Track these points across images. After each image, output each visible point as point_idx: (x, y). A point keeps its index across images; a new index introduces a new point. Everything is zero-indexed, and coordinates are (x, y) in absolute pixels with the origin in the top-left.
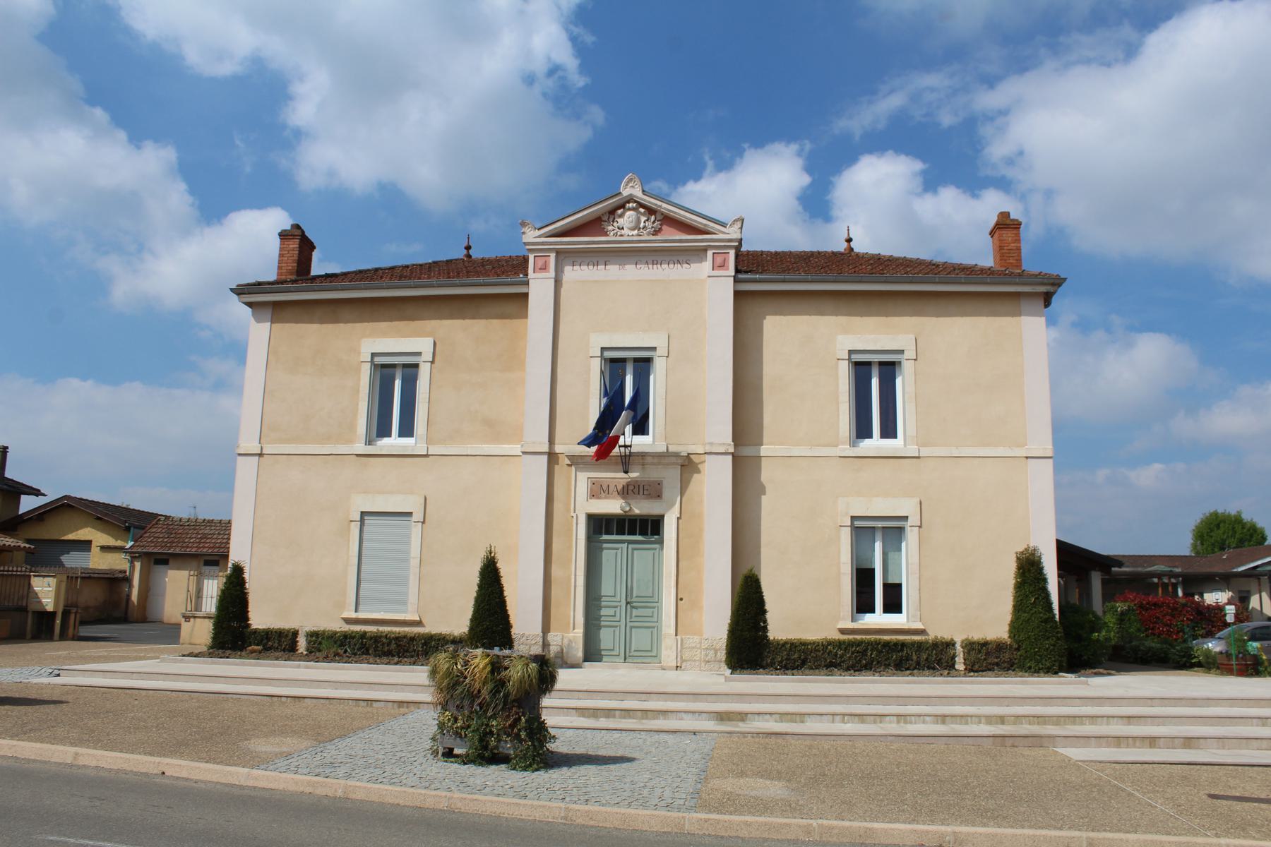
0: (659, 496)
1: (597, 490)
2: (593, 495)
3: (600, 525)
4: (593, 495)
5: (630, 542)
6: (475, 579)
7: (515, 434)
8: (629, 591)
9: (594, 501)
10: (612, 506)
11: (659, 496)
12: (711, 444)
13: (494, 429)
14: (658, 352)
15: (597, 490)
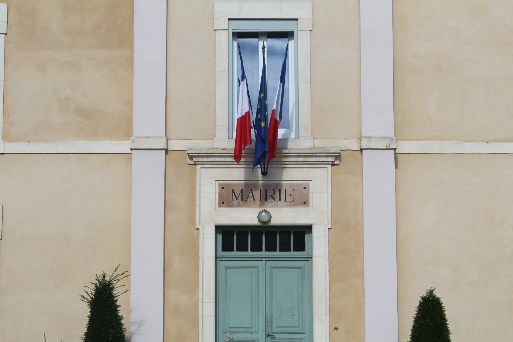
0: (305, 203)
1: (229, 196)
2: (223, 202)
3: (230, 238)
4: (223, 202)
5: (268, 259)
6: (84, 312)
7: (125, 127)
8: (268, 322)
9: (224, 209)
10: (246, 216)
11: (305, 203)
12: (369, 137)
13: (91, 120)
14: (301, 25)
15: (229, 196)
